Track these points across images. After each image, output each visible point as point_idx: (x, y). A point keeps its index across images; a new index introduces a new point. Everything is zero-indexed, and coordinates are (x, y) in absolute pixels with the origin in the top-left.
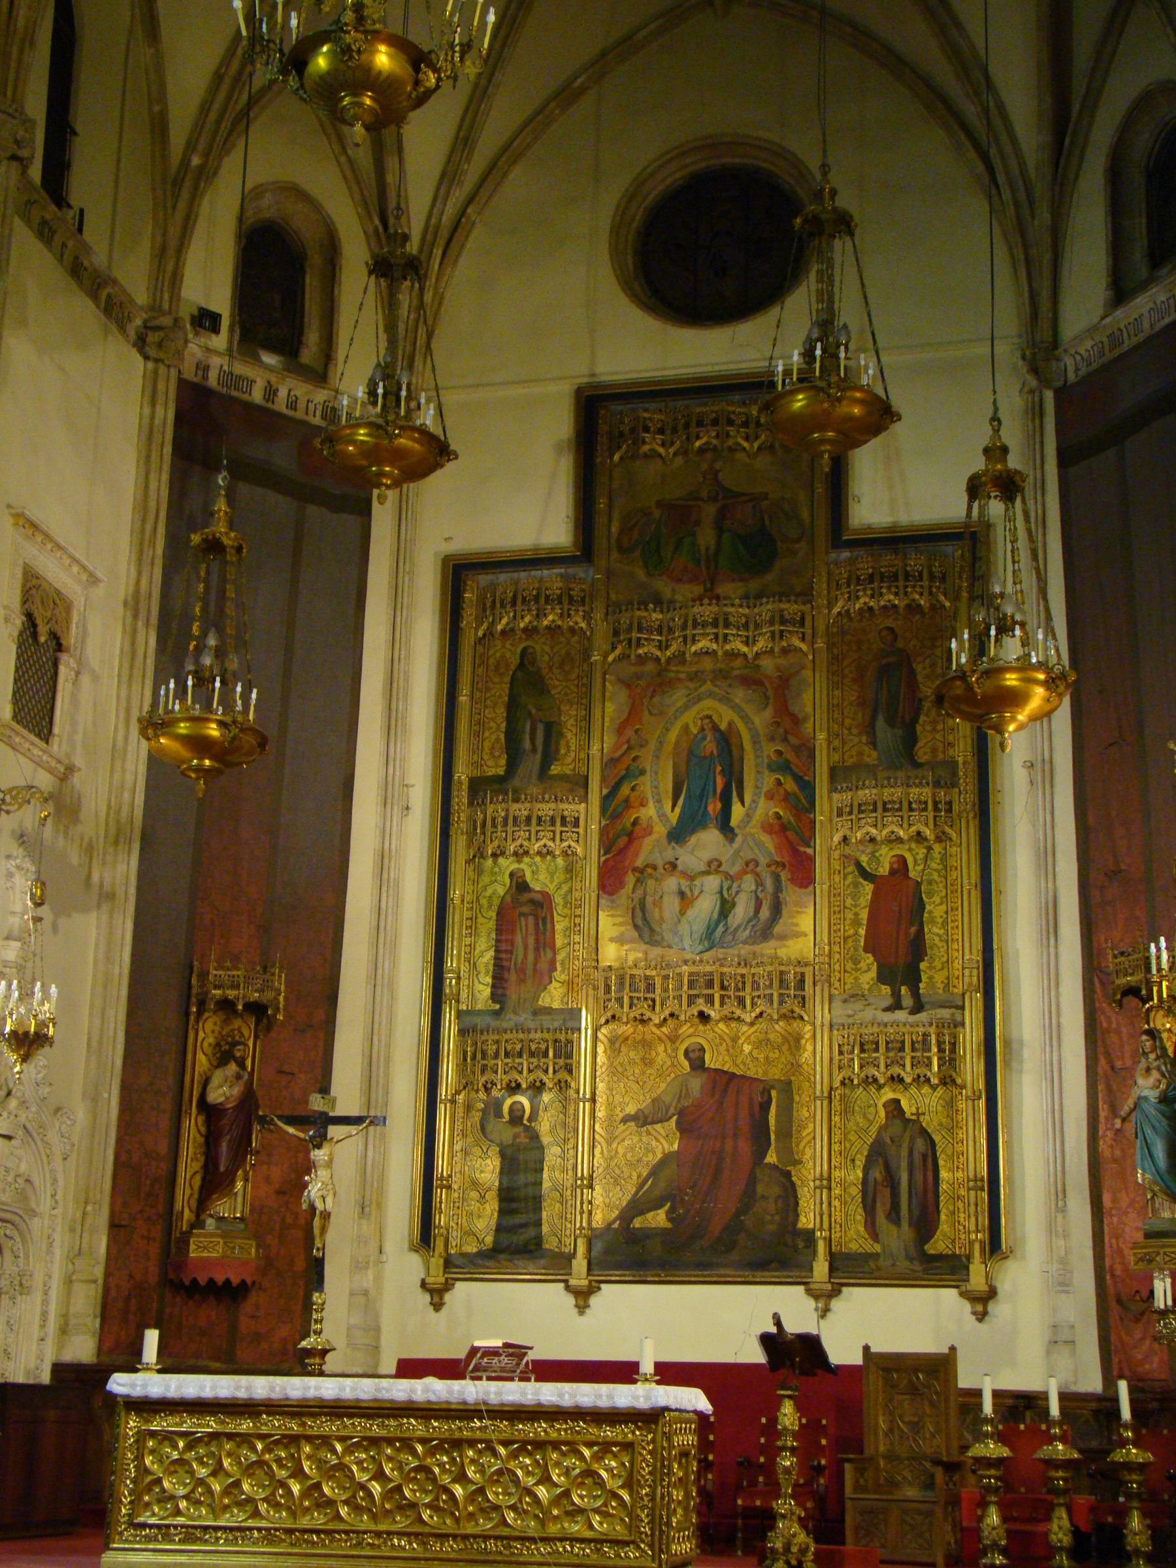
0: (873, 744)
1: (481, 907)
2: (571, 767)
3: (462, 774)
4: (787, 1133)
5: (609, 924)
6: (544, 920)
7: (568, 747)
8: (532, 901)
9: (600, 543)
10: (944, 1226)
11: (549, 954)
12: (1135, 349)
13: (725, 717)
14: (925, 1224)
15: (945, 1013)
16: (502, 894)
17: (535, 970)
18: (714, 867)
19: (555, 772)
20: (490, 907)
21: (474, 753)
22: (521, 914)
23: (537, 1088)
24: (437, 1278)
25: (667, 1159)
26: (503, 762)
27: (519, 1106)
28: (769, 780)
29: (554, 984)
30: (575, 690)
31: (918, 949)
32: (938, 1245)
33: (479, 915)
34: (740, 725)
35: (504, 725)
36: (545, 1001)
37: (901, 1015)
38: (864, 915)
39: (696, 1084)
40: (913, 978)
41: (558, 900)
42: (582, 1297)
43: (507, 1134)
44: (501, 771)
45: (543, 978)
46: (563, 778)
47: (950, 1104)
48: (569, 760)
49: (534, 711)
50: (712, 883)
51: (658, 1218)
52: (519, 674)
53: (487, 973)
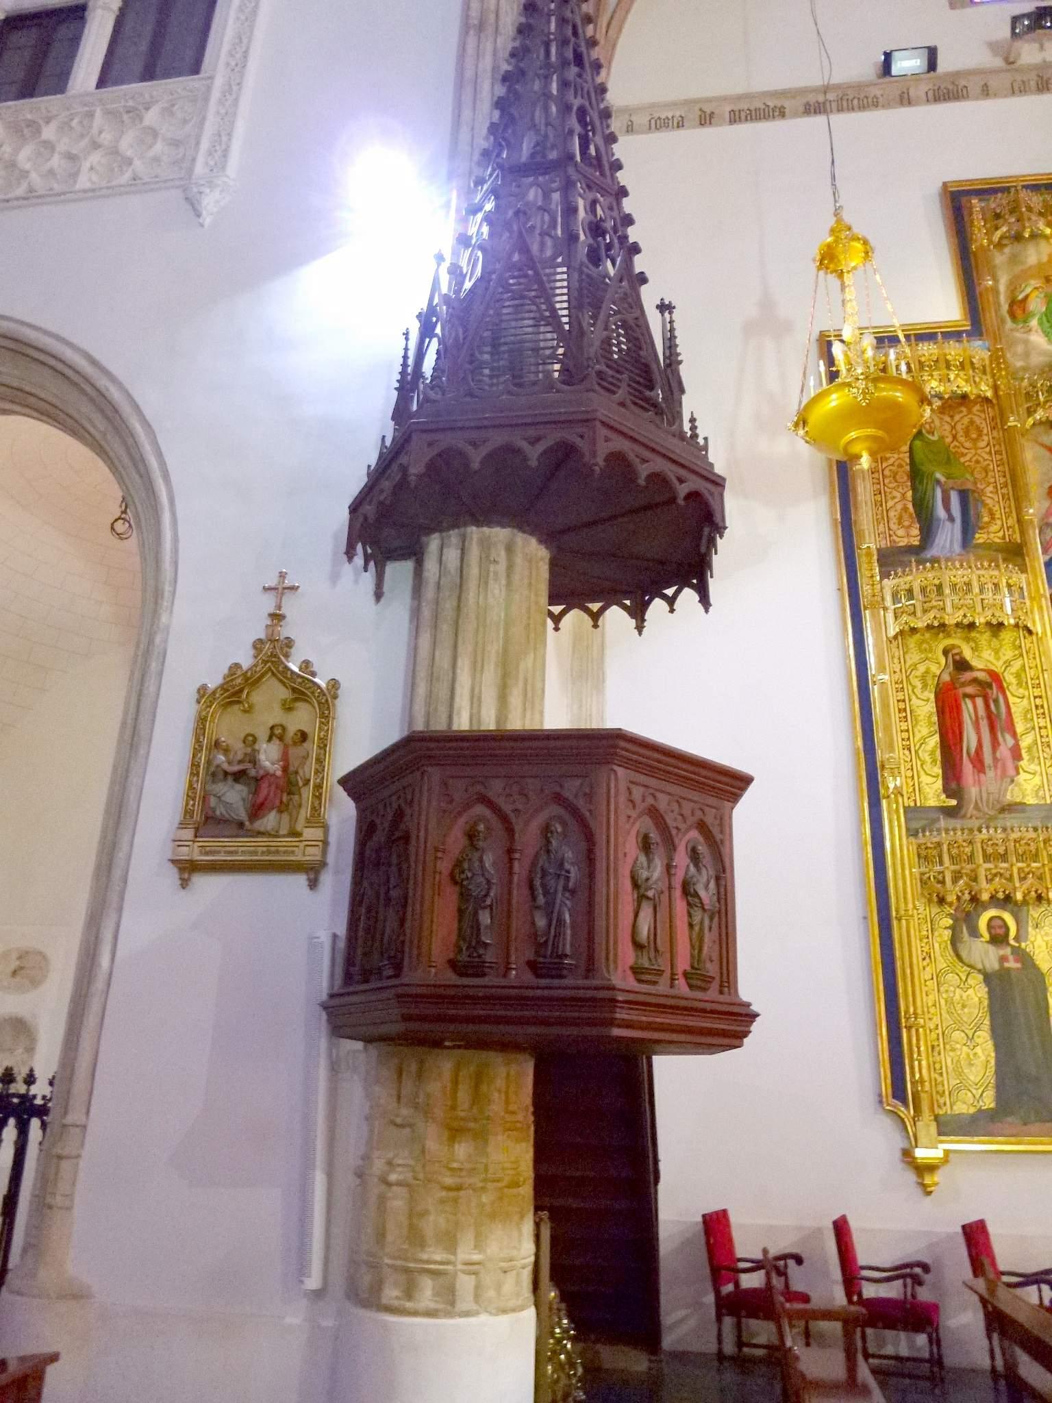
1: (914, 687)
2: (1001, 534)
3: (870, 543)
6: (996, 701)
7: (992, 514)
8: (975, 681)
9: (990, 318)
11: (1010, 741)
16: (938, 673)
17: (995, 759)
19: (981, 541)
20: (925, 686)
21: (879, 523)
22: (966, 696)
26: (915, 531)
27: (999, 922)
29: (1023, 776)
30: (986, 457)
33: (913, 697)
35: (910, 494)
41: (1009, 678)
44: (916, 542)
46: (988, 546)
48: (994, 528)
49: (943, 479)
52: (918, 443)
53: (934, 761)
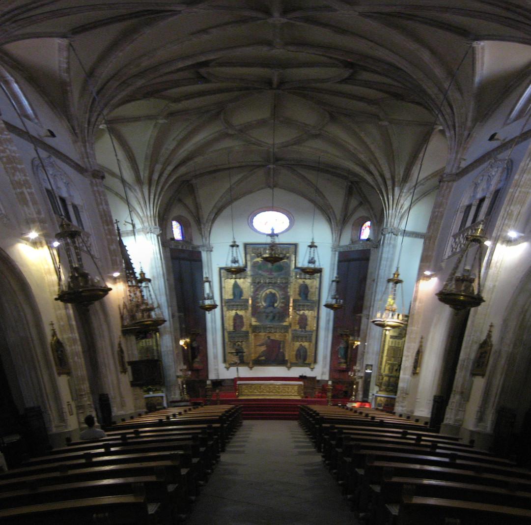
0: (300, 296)
4: (284, 347)
5: (253, 320)
10: (308, 359)
13: (273, 291)
14: (305, 359)
18: (272, 312)
23: (242, 342)
24: (228, 366)
25: (264, 351)
31: (306, 325)
32: (307, 362)
34: (276, 293)
36: (242, 330)
37: (302, 333)
39: (269, 341)
40: (305, 328)
42: (251, 368)
47: (310, 345)
50: (271, 314)
51: (263, 358)
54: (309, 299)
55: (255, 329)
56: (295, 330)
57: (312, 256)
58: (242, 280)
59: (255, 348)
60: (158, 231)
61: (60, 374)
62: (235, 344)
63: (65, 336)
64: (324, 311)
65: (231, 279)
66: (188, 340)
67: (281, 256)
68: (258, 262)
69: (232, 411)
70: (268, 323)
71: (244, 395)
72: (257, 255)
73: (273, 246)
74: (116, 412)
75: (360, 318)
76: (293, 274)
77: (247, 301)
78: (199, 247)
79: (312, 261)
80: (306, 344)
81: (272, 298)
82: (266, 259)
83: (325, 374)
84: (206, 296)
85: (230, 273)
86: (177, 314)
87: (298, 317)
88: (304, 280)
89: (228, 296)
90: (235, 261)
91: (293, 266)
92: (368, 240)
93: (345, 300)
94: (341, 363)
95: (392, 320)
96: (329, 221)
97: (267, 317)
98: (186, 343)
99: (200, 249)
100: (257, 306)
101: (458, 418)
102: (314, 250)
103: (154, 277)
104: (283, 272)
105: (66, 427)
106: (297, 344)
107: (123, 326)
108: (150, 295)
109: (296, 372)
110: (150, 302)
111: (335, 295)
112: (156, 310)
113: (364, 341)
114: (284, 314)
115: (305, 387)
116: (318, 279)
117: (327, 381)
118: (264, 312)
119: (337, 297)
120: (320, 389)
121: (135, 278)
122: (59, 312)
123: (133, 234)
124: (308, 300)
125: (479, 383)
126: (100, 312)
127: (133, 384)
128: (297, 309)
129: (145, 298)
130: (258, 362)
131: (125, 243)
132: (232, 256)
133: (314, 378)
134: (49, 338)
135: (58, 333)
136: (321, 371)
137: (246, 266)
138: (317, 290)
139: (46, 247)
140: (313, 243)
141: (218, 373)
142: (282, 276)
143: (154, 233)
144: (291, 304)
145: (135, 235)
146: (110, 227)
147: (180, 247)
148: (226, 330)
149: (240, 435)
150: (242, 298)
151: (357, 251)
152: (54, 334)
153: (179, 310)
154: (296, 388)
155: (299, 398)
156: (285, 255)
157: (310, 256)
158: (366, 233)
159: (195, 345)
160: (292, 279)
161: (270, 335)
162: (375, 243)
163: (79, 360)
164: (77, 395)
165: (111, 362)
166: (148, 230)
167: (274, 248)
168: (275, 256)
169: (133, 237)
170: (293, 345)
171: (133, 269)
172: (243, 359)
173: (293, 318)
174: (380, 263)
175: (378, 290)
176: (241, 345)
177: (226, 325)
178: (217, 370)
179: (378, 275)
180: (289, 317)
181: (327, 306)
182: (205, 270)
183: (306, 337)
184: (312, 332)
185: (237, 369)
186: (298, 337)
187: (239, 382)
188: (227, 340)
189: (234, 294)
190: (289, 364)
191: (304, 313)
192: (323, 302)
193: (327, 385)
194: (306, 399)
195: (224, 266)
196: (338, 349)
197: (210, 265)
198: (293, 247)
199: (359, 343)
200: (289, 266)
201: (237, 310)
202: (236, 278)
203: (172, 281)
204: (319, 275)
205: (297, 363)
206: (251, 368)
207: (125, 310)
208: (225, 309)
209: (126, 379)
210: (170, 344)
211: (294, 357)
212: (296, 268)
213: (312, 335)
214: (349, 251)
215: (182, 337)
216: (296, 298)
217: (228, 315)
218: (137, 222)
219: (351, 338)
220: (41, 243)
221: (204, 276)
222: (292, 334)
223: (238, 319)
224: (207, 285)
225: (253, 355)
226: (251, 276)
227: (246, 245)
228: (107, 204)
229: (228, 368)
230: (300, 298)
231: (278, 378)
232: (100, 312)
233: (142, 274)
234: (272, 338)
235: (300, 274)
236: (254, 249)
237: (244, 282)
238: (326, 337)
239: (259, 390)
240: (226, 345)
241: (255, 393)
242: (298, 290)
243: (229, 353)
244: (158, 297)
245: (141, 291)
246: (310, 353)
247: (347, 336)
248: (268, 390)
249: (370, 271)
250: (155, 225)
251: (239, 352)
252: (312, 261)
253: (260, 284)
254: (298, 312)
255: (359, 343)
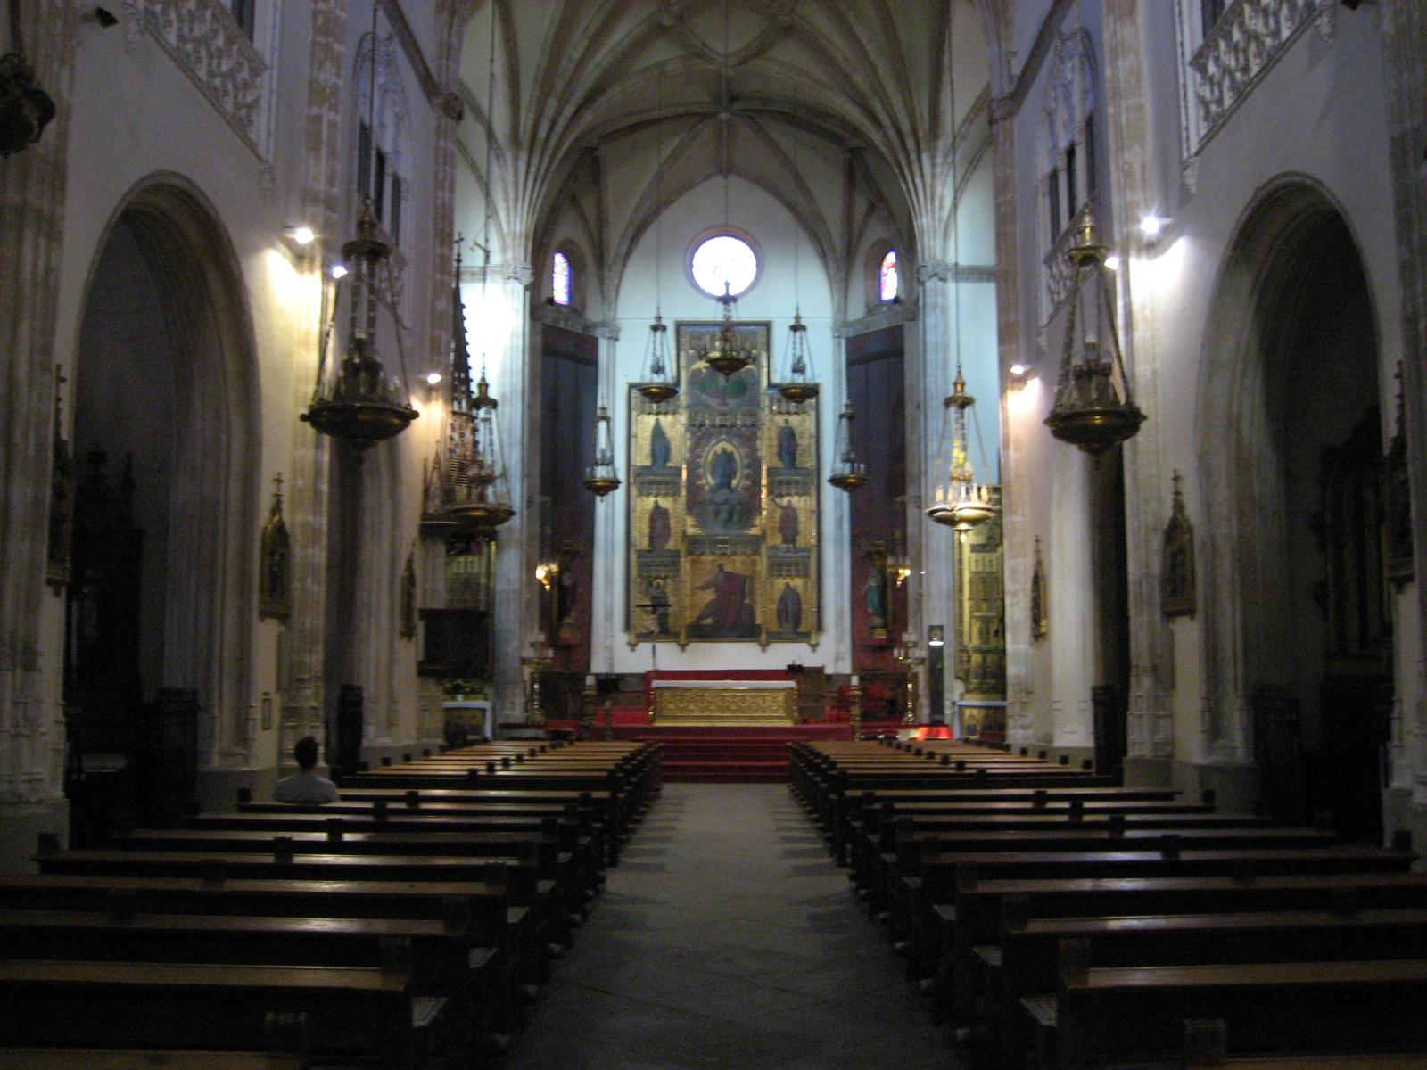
0: (781, 460)
4: (752, 593)
5: (690, 521)
10: (803, 624)
12: (875, 332)
13: (730, 448)
14: (797, 623)
15: (804, 554)
18: (726, 501)
23: (665, 578)
24: (634, 640)
25: (711, 602)
28: (747, 471)
31: (796, 532)
32: (801, 630)
37: (789, 555)
38: (778, 520)
39: (721, 577)
40: (794, 542)
42: (683, 647)
43: (654, 592)
45: (667, 538)
47: (806, 584)
50: (726, 507)
51: (709, 621)
54: (798, 465)
55: (693, 544)
56: (774, 547)
57: (798, 353)
58: (670, 417)
59: (693, 593)
60: (527, 277)
61: (264, 615)
62: (650, 584)
63: (299, 518)
64: (830, 494)
65: (649, 414)
66: (554, 568)
67: (742, 355)
68: (699, 370)
69: (640, 758)
70: (719, 531)
71: (667, 717)
72: (699, 353)
73: (727, 329)
74: (375, 737)
75: (904, 504)
76: (765, 401)
77: (678, 471)
78: (595, 325)
79: (798, 368)
80: (797, 583)
81: (725, 465)
82: (714, 363)
83: (843, 659)
84: (599, 456)
85: (647, 399)
86: (538, 498)
87: (779, 513)
88: (786, 417)
89: (642, 459)
90: (658, 369)
91: (765, 383)
92: (896, 300)
93: (868, 464)
94: (875, 627)
95: (968, 505)
96: (823, 256)
97: (717, 513)
98: (549, 575)
99: (598, 333)
100: (698, 486)
101: (1160, 736)
102: (801, 338)
103: (503, 396)
104: (746, 397)
105: (246, 759)
106: (780, 583)
107: (425, 515)
108: (491, 444)
109: (781, 655)
110: (488, 461)
111: (848, 453)
112: (498, 482)
113: (917, 566)
114: (749, 507)
115: (801, 694)
116: (813, 413)
117: (848, 677)
118: (712, 502)
119: (853, 456)
120: (834, 698)
121: (469, 393)
122: (301, 452)
123: (481, 277)
124: (797, 469)
125: (1188, 633)
126: (384, 471)
127: (424, 670)
128: (776, 491)
129: (480, 448)
130: (700, 632)
131: (464, 299)
132: (654, 354)
133: (819, 671)
134: (263, 517)
135: (285, 506)
136: (831, 652)
137: (677, 383)
138: (813, 441)
139: (318, 274)
140: (798, 318)
141: (611, 658)
142: (745, 408)
143: (520, 283)
144: (764, 482)
145: (484, 280)
146: (446, 251)
147: (562, 325)
148: (635, 545)
149: (655, 821)
150: (669, 464)
151: (881, 331)
152: (276, 509)
153: (544, 490)
154: (781, 698)
155: (788, 723)
156: (750, 352)
157: (794, 355)
158: (890, 285)
159: (567, 582)
160: (764, 416)
161: (724, 560)
162: (909, 307)
163: (316, 587)
164: (290, 680)
165: (385, 604)
166: (510, 272)
167: (729, 335)
168: (728, 354)
169: (480, 285)
170: (772, 585)
171: (467, 369)
172: (666, 623)
173: (770, 517)
174: (925, 358)
175: (929, 428)
176: (664, 587)
177: (635, 534)
178: (609, 649)
179: (925, 390)
180: (760, 513)
181: (837, 481)
182: (602, 390)
183: (797, 565)
184: (807, 550)
185: (654, 647)
186: (780, 565)
187: (655, 683)
188: (634, 572)
189: (653, 454)
190: (764, 637)
191: (789, 501)
192: (827, 473)
193: (849, 687)
194: (806, 726)
195: (636, 379)
196: (866, 593)
197: (611, 375)
198: (762, 330)
199: (907, 572)
200: (758, 383)
201: (657, 496)
202: (658, 414)
203: (538, 411)
204: (813, 401)
205: (780, 633)
206: (683, 647)
207: (436, 475)
208: (634, 492)
209: (410, 653)
210: (515, 572)
211: (775, 619)
212: (771, 386)
213: (809, 557)
214: (865, 334)
215: (543, 559)
216: (773, 466)
217: (638, 509)
218: (495, 246)
219: (890, 561)
220: (312, 260)
221: (600, 404)
222: (769, 557)
223: (659, 515)
224: (602, 426)
225: (688, 613)
226: (688, 406)
227: (680, 326)
228: (452, 190)
229: (633, 646)
230: (780, 465)
231: (738, 678)
232: (384, 471)
233: (484, 385)
234: (728, 568)
235: (779, 402)
236: (693, 336)
237: (673, 425)
238: (839, 561)
239: (699, 704)
240: (632, 584)
241: (692, 711)
242: (775, 442)
243: (638, 606)
244: (506, 450)
245: (475, 430)
246: (808, 607)
247: (882, 556)
248: (719, 704)
249: (908, 382)
250: (525, 260)
251: (658, 605)
252: (798, 368)
253: (703, 429)
254: (778, 500)
255: (907, 572)
